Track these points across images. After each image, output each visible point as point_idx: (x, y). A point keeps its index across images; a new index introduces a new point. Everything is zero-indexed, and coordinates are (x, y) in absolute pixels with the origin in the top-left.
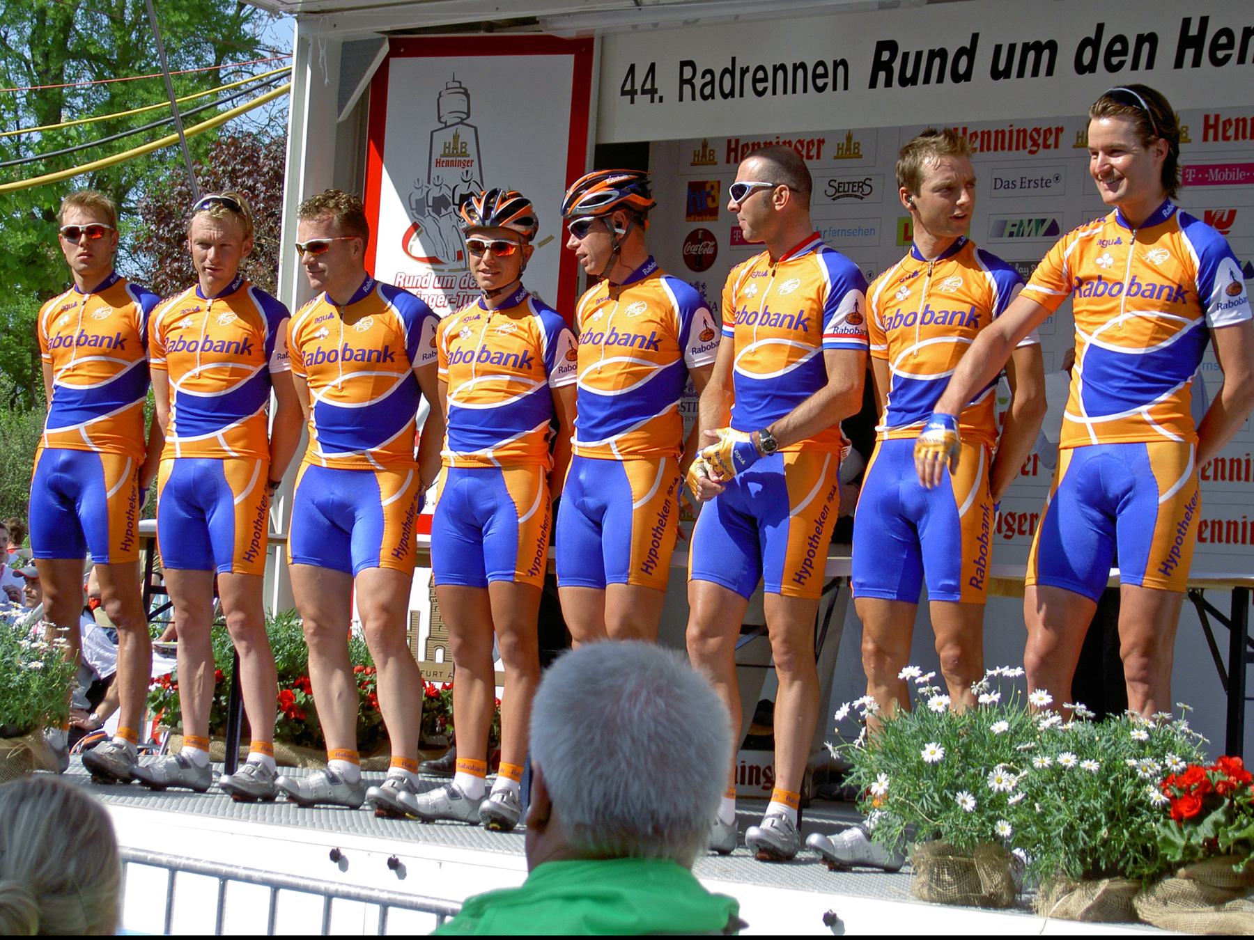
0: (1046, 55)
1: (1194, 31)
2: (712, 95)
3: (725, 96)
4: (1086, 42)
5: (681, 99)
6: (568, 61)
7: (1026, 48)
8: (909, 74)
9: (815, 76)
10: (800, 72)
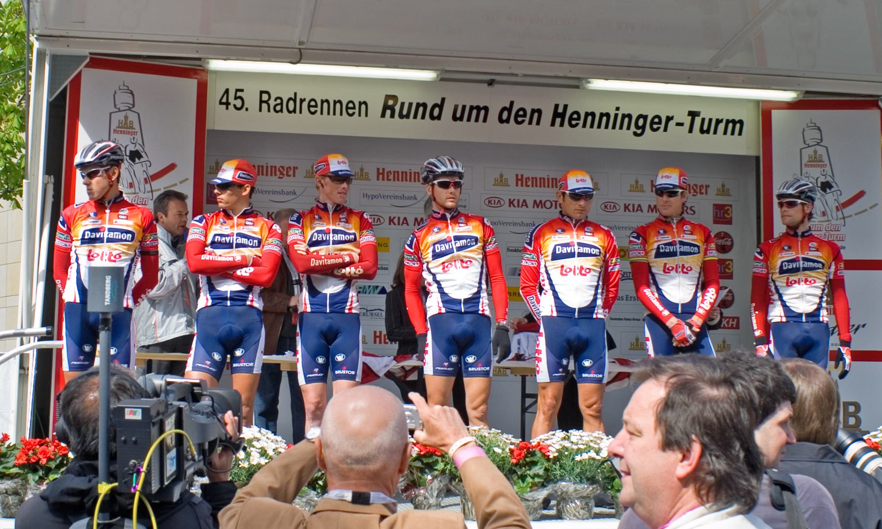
0: (483, 112)
1: (560, 110)
2: (281, 111)
3: (290, 112)
4: (504, 109)
5: (260, 110)
6: (192, 84)
7: (472, 108)
8: (405, 112)
9: (347, 108)
10: (338, 105)
